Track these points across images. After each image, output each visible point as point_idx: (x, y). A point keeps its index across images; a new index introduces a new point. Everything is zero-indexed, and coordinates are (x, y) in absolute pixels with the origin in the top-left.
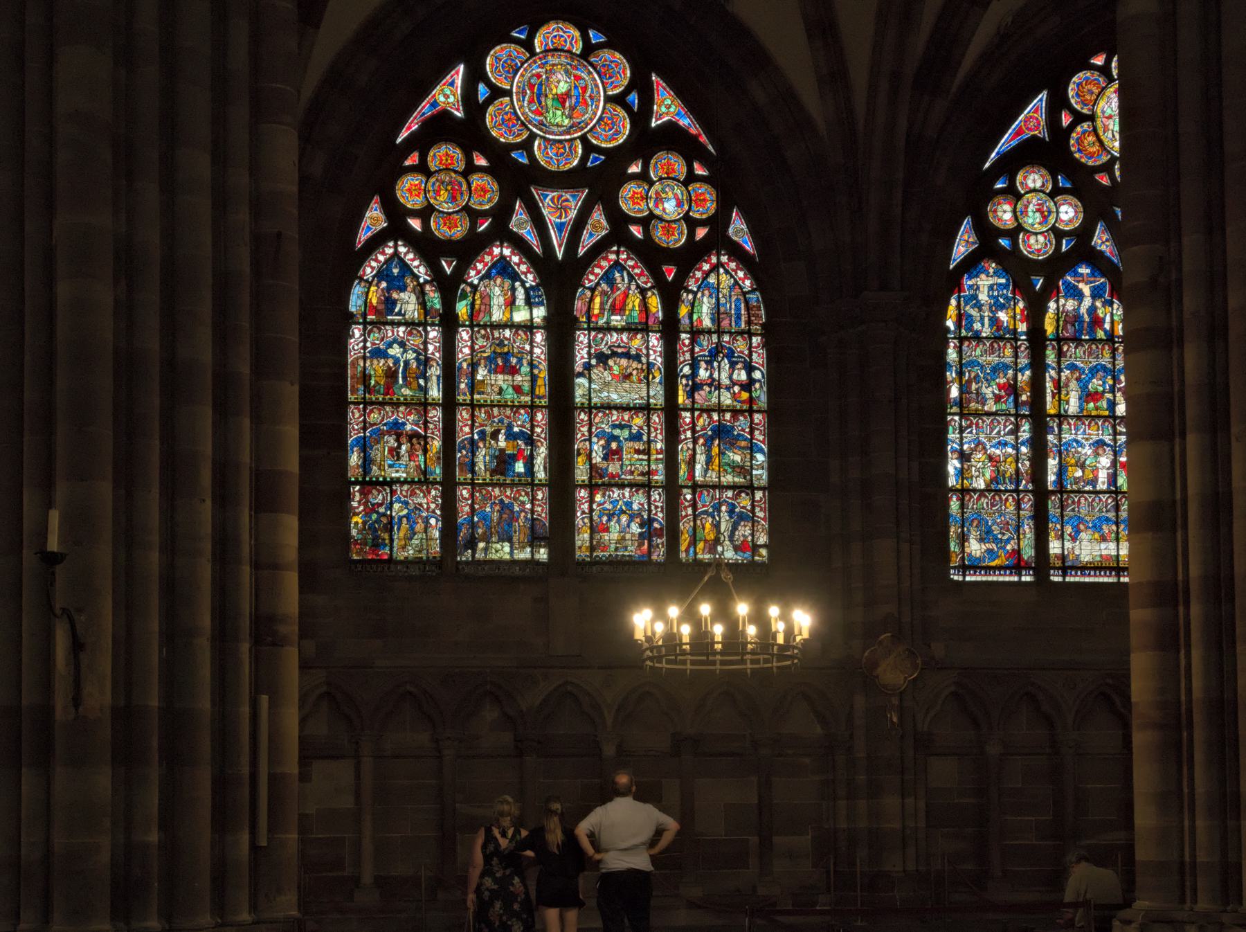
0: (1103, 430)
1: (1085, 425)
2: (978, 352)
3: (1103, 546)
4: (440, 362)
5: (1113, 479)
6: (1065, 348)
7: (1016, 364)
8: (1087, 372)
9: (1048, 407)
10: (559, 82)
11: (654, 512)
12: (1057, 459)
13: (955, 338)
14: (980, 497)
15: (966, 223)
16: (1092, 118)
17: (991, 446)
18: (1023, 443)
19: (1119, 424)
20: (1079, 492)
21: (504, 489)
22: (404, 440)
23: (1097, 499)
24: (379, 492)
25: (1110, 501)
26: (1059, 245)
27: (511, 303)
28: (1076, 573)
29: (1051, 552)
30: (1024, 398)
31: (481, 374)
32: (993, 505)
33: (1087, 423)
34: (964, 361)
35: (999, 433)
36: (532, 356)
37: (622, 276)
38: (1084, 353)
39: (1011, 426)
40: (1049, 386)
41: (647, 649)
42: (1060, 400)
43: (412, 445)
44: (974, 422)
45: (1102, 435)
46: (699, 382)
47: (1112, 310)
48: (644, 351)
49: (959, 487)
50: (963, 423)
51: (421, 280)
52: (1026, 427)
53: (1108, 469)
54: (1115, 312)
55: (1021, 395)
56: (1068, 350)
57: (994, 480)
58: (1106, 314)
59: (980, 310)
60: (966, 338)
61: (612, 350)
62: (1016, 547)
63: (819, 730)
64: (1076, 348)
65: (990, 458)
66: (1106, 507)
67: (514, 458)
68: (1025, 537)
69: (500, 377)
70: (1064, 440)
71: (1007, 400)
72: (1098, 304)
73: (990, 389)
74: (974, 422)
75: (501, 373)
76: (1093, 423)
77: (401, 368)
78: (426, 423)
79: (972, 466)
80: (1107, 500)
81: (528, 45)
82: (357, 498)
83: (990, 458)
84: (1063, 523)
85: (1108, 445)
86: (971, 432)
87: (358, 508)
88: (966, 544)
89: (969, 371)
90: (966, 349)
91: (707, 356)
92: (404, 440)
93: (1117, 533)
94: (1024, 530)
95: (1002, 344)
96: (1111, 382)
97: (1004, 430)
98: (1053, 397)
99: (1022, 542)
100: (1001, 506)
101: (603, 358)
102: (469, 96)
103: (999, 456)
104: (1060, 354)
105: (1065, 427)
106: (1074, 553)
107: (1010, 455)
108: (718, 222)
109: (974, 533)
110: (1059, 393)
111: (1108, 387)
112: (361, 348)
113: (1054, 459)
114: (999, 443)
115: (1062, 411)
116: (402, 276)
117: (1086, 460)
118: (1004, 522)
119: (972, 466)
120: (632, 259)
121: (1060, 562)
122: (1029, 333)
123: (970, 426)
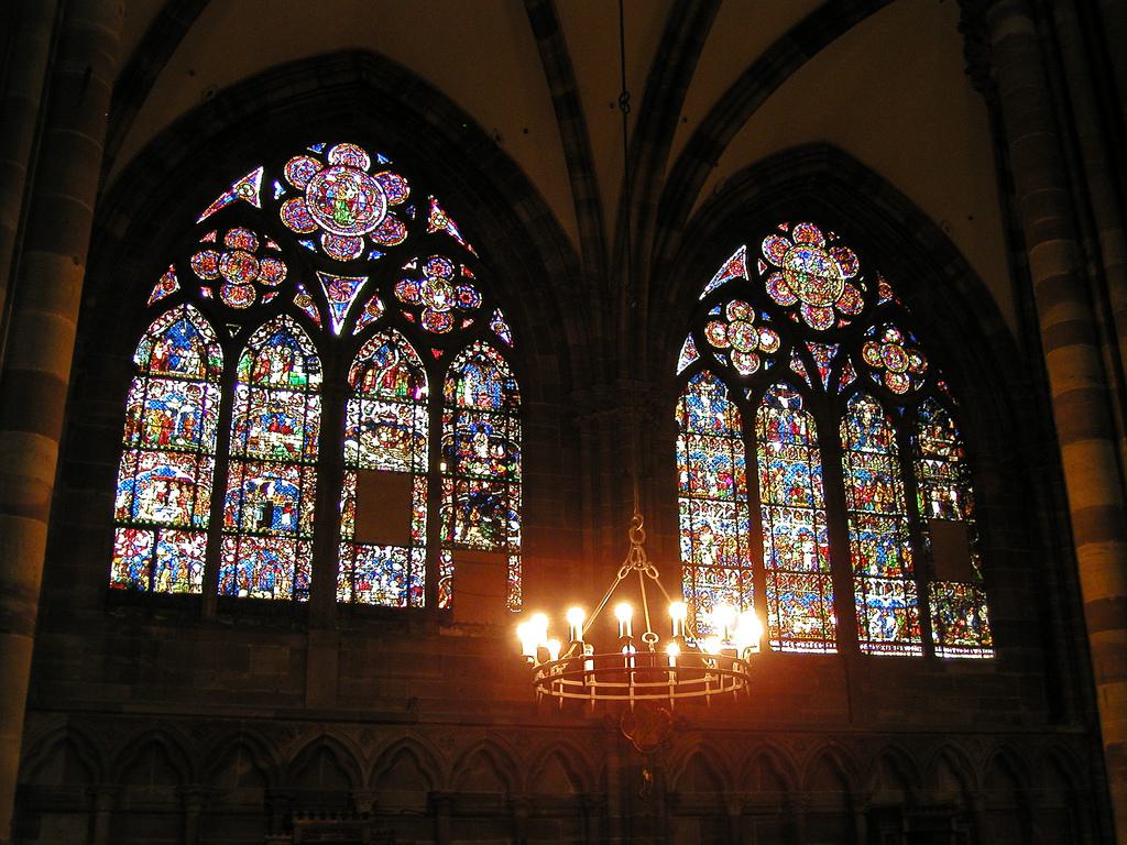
15: (689, 341)
22: (174, 486)
24: (144, 535)
27: (289, 367)
37: (394, 354)
41: (539, 668)
63: (572, 791)
81: (323, 158)
82: (122, 539)
92: (174, 486)
101: (373, 427)
102: (267, 190)
108: (482, 316)
120: (403, 341)
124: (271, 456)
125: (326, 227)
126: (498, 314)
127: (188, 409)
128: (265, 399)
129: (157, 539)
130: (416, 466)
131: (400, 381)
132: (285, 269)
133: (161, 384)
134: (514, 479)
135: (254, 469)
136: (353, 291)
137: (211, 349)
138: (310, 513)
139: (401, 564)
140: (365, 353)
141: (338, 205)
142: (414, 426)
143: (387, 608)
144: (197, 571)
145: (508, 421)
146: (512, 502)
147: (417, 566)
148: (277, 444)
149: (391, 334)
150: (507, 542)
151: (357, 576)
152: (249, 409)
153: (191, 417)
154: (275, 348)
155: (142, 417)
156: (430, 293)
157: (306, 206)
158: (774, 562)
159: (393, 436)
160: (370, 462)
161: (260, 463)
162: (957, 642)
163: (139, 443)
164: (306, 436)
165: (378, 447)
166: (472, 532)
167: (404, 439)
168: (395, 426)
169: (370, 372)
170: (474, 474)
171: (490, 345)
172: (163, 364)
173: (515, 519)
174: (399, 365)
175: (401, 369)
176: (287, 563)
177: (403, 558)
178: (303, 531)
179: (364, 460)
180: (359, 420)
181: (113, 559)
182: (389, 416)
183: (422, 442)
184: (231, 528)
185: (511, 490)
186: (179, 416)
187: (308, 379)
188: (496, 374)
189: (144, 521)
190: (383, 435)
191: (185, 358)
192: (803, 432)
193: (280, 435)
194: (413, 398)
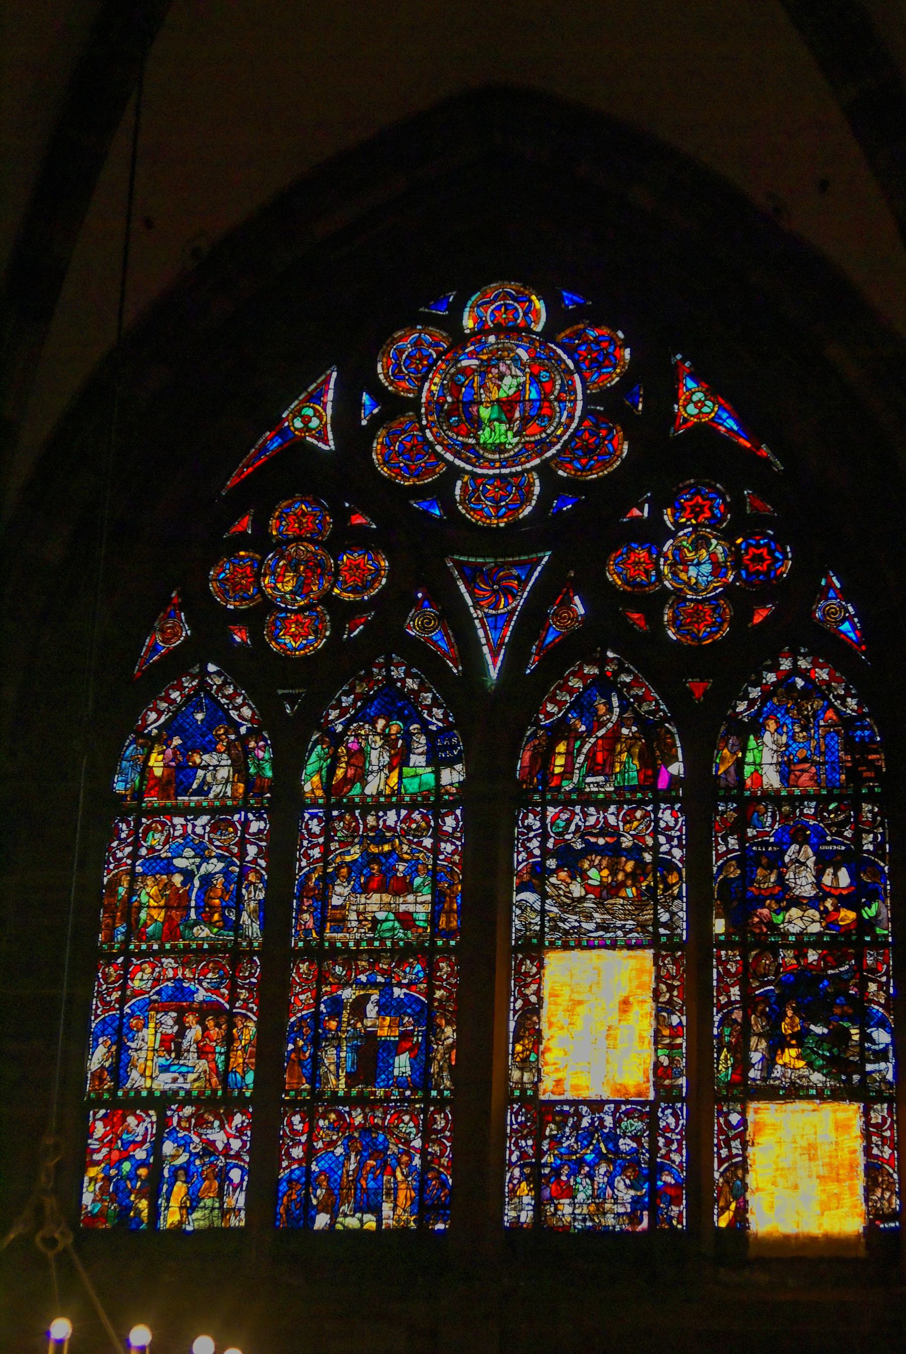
4: (266, 877)
10: (501, 377)
11: (663, 1152)
21: (372, 1110)
31: (340, 894)
36: (436, 859)
43: (205, 1029)
46: (756, 892)
48: (650, 841)
51: (243, 730)
61: (587, 842)
67: (395, 1049)
69: (376, 897)
75: (376, 892)
77: (195, 890)
78: (233, 988)
81: (453, 324)
82: (100, 1129)
87: (98, 1151)
91: (772, 844)
112: (128, 857)
116: (210, 723)
120: (628, 672)
124: (370, 941)
125: (462, 464)
126: (830, 585)
127: (214, 866)
128: (357, 828)
129: (163, 1122)
130: (662, 931)
131: (624, 757)
132: (385, 564)
133: (163, 824)
134: (875, 936)
135: (338, 969)
136: (523, 583)
137: (252, 744)
138: (450, 1048)
139: (636, 1138)
140: (550, 708)
141: (485, 413)
142: (657, 844)
143: (607, 1232)
144: (236, 1180)
145: (858, 811)
146: (873, 987)
147: (669, 1142)
148: (381, 916)
149: (602, 662)
150: (865, 1074)
151: (547, 1171)
152: (326, 851)
153: (219, 881)
154: (373, 724)
155: (132, 892)
156: (680, 561)
157: (422, 429)
159: (613, 873)
160: (566, 932)
161: (350, 957)
163: (126, 942)
164: (438, 898)
165: (582, 899)
166: (786, 1059)
167: (634, 877)
168: (614, 851)
169: (561, 748)
170: (786, 934)
171: (813, 654)
172: (166, 786)
173: (882, 1023)
174: (621, 723)
175: (625, 731)
176: (406, 1153)
177: (639, 1125)
178: (437, 1087)
179: (555, 928)
180: (542, 846)
181: (84, 1172)
182: (602, 833)
183: (673, 879)
184: (299, 1092)
185: (870, 961)
186: (197, 883)
187: (438, 779)
188: (830, 714)
189: (138, 1092)
190: (593, 873)
191: (205, 768)
193: (386, 898)
194: (653, 787)
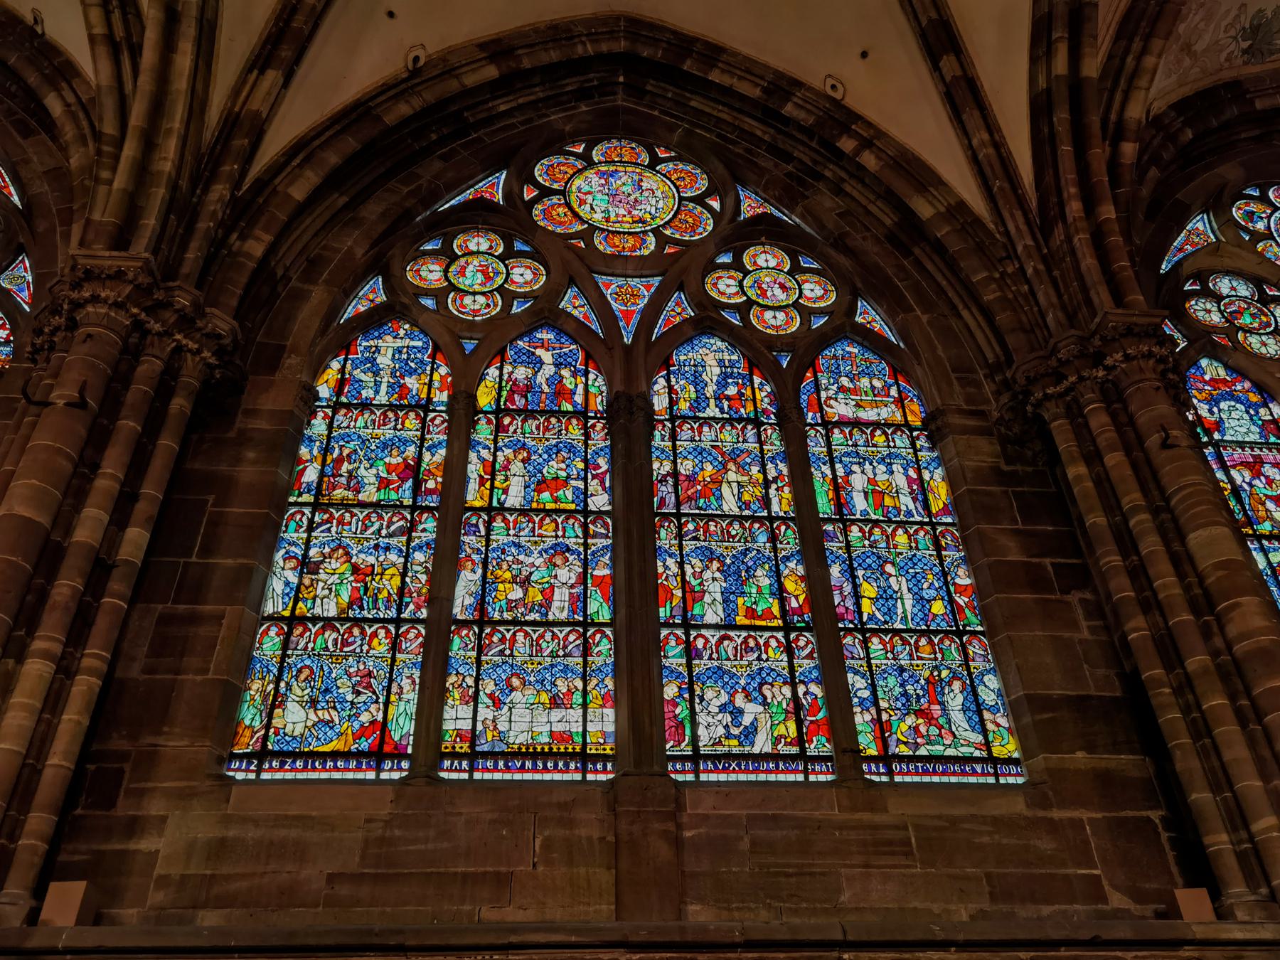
0: (564, 530)
1: (534, 523)
2: (360, 422)
3: (556, 714)
5: (578, 602)
6: (507, 421)
7: (422, 439)
8: (540, 451)
9: (469, 497)
12: (480, 571)
13: (328, 407)
14: (323, 629)
16: (563, 193)
17: (360, 552)
18: (420, 548)
19: (593, 522)
20: (515, 622)
23: (548, 636)
25: (572, 638)
26: (507, 306)
28: (496, 764)
29: (448, 726)
30: (431, 484)
32: (345, 643)
33: (537, 520)
34: (334, 434)
35: (379, 530)
38: (538, 428)
39: (401, 523)
40: (474, 469)
42: (492, 488)
44: (337, 515)
45: (564, 536)
47: (587, 380)
49: (287, 613)
50: (317, 519)
52: (430, 524)
53: (572, 587)
54: (590, 383)
55: (426, 481)
56: (511, 423)
57: (355, 601)
58: (576, 386)
59: (376, 374)
60: (348, 406)
62: (380, 717)
64: (524, 421)
65: (356, 569)
66: (565, 647)
68: (400, 699)
70: (494, 545)
71: (399, 487)
72: (565, 373)
73: (374, 471)
74: (337, 515)
76: (548, 520)
79: (318, 580)
80: (567, 635)
83: (356, 569)
84: (478, 674)
85: (573, 552)
86: (329, 530)
88: (278, 711)
89: (341, 447)
90: (341, 418)
93: (585, 693)
94: (401, 688)
95: (401, 414)
96: (581, 465)
97: (388, 527)
98: (482, 482)
99: (391, 709)
100: (361, 645)
103: (373, 566)
104: (499, 428)
105: (498, 524)
106: (495, 728)
107: (394, 565)
109: (299, 692)
110: (493, 479)
111: (575, 472)
113: (473, 571)
114: (376, 547)
115: (495, 503)
117: (531, 573)
118: (366, 672)
119: (318, 580)
121: (466, 745)
122: (451, 405)
123: (329, 521)
158: (481, 605)
162: (923, 751)
192: (579, 398)
